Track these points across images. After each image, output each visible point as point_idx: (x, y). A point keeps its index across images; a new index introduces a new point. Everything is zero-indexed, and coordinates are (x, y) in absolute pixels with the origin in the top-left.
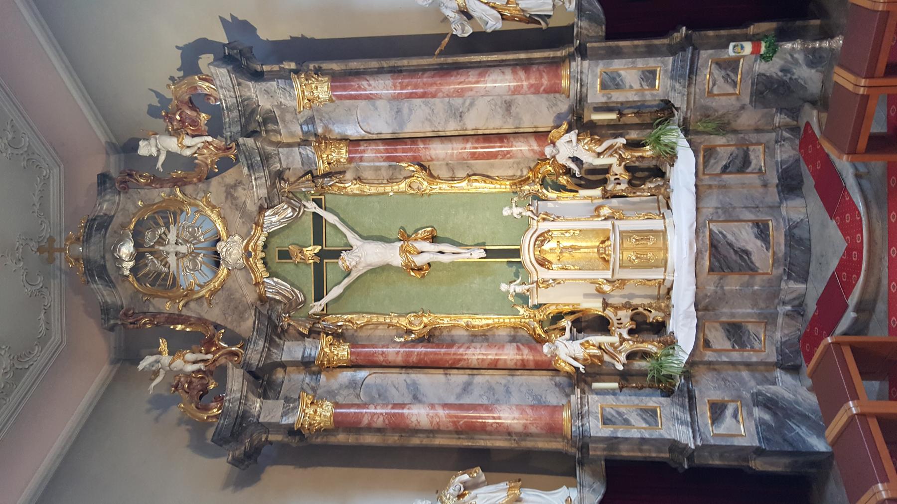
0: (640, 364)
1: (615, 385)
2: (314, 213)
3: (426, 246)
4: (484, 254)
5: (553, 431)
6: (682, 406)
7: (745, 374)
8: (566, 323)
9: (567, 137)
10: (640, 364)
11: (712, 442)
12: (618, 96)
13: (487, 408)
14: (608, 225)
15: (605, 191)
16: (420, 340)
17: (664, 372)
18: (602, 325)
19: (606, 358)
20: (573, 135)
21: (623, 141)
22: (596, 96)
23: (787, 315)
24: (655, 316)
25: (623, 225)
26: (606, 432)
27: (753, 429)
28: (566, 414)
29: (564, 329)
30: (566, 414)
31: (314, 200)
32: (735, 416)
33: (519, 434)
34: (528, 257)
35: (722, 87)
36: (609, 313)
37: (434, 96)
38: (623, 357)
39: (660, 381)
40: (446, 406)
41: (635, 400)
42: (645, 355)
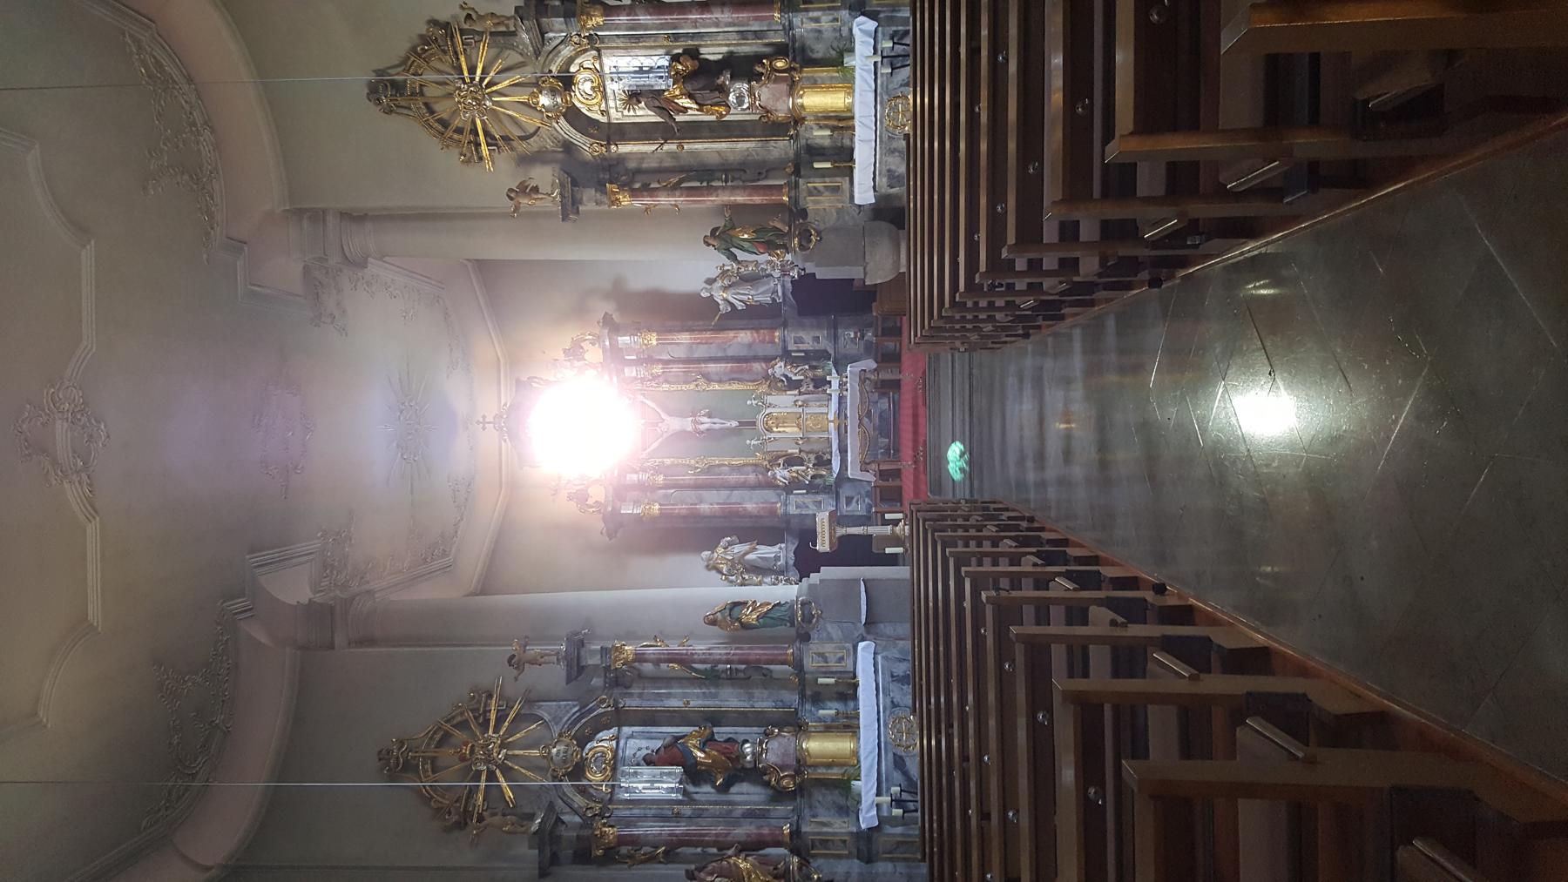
0: (818, 481)
1: (804, 491)
3: (706, 419)
4: (738, 424)
5: (773, 512)
8: (781, 461)
9: (779, 365)
10: (818, 481)
11: (845, 514)
12: (802, 347)
14: (801, 410)
16: (703, 472)
17: (827, 484)
18: (801, 462)
19: (800, 478)
21: (807, 367)
22: (791, 347)
23: (881, 453)
24: (826, 457)
25: (807, 410)
26: (797, 512)
27: (864, 507)
28: (779, 505)
29: (780, 464)
30: (779, 505)
32: (857, 502)
33: (756, 516)
34: (760, 426)
35: (854, 346)
36: (803, 455)
37: (711, 343)
38: (809, 478)
40: (718, 504)
41: (812, 496)
42: (822, 476)
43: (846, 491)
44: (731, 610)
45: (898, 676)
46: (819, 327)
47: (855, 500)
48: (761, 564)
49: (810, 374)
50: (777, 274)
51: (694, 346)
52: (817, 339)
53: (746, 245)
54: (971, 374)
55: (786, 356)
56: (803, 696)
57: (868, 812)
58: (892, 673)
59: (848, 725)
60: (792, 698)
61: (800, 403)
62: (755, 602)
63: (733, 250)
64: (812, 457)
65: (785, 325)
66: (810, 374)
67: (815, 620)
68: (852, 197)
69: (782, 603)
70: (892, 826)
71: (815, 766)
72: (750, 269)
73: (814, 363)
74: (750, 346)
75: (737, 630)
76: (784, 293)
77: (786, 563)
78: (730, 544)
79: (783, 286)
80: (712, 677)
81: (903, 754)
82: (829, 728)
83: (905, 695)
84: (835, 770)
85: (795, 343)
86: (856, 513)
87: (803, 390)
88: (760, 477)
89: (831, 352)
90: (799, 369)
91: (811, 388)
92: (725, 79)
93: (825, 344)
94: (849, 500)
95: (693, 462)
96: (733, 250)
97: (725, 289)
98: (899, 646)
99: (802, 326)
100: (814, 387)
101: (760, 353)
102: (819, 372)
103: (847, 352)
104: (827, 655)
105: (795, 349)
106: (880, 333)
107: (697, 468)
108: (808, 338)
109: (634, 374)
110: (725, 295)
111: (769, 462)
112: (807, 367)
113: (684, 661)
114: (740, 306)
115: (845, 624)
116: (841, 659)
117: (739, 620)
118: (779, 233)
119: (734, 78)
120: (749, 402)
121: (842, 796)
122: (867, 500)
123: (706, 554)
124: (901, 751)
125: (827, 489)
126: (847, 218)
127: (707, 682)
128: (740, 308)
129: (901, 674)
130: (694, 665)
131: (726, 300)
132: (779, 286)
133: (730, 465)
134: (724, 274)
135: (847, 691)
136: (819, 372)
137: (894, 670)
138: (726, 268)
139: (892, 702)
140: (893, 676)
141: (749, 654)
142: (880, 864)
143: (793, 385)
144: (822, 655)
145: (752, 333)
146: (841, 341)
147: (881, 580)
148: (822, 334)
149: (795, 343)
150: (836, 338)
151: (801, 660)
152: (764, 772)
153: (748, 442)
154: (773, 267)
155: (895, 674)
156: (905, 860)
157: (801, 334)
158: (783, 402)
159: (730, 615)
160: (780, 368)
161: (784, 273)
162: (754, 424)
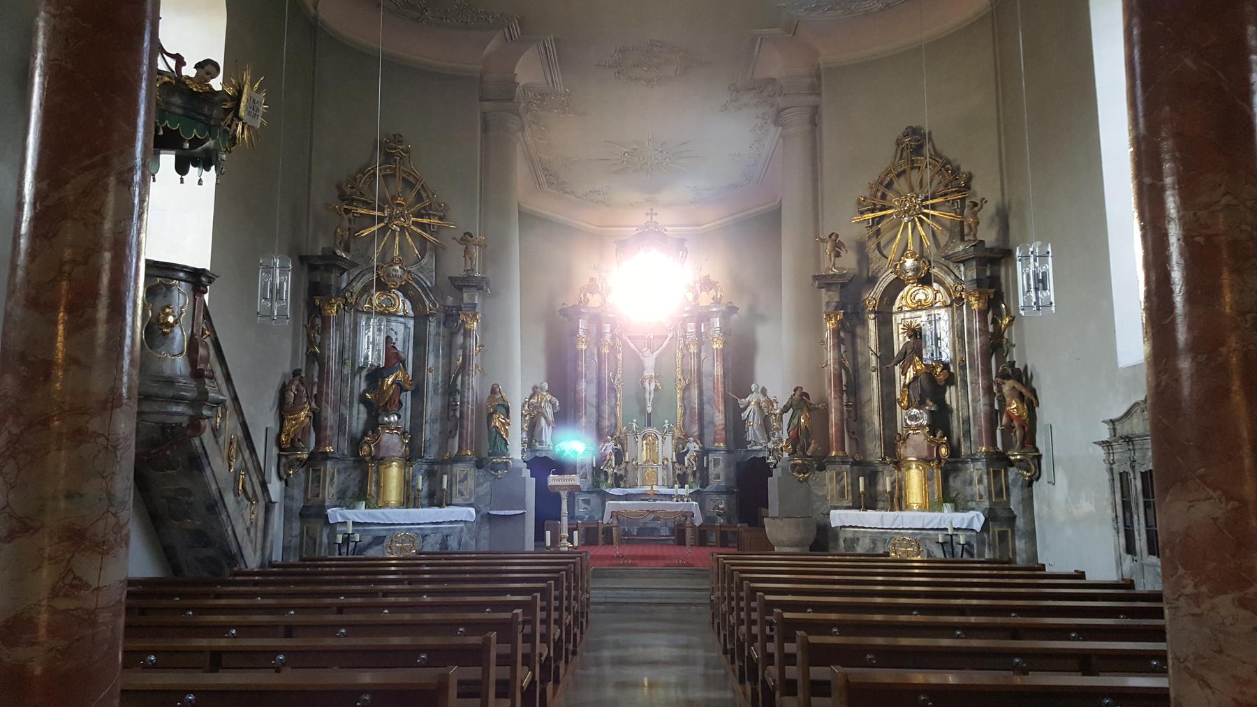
2: (667, 336)
3: (653, 387)
4: (649, 412)
6: (589, 489)
7: (600, 515)
8: (619, 447)
9: (697, 446)
10: (603, 476)
11: (576, 499)
12: (711, 465)
13: (585, 413)
14: (660, 463)
15: (675, 462)
18: (618, 462)
19: (605, 462)
20: (697, 449)
21: (695, 469)
23: (624, 529)
24: (622, 484)
25: (660, 469)
27: (581, 514)
31: (673, 336)
32: (585, 508)
34: (647, 430)
36: (623, 465)
37: (714, 392)
38: (605, 469)
39: (597, 482)
40: (585, 396)
42: (607, 480)
43: (595, 500)
44: (503, 406)
45: (447, 540)
46: (728, 479)
47: (587, 506)
48: (537, 430)
49: (689, 471)
50: (770, 445)
51: (712, 378)
52: (718, 477)
53: (795, 421)
54: (691, 604)
55: (704, 452)
56: (433, 463)
57: (340, 514)
58: (450, 535)
59: (409, 500)
60: (432, 454)
61: (666, 463)
62: (509, 425)
63: (791, 410)
64: (622, 472)
65: (729, 451)
66: (689, 471)
67: (493, 472)
68: (836, 508)
70: (328, 534)
71: (378, 472)
72: (775, 424)
73: (698, 475)
74: (712, 423)
75: (487, 409)
76: (754, 450)
77: (537, 450)
78: (554, 405)
79: (760, 450)
80: (450, 390)
81: (385, 544)
82: (407, 484)
83: (432, 546)
84: (374, 488)
85: (715, 459)
86: (576, 507)
87: (676, 465)
88: (607, 430)
89: (707, 489)
90: (694, 463)
91: (678, 472)
92: (930, 406)
93: (714, 484)
94: (587, 502)
95: (619, 376)
96: (791, 410)
97: (758, 403)
99: (728, 465)
100: (679, 474)
101: (706, 431)
102: (691, 479)
103: (707, 502)
104: (466, 483)
105: (710, 460)
106: (723, 529)
107: (614, 379)
108: (719, 472)
109: (689, 330)
110: (753, 403)
111: (619, 437)
112: (695, 469)
113: (464, 368)
114: (744, 415)
115: (489, 497)
116: (462, 494)
117: (495, 412)
118: (804, 449)
119: (931, 413)
120: (666, 421)
121: (353, 494)
122: (587, 516)
123: (546, 386)
124: (387, 542)
125: (596, 483)
126: (818, 503)
127: (447, 386)
128: (742, 415)
129: (449, 543)
130: (460, 377)
131: (749, 404)
132: (759, 447)
133: (616, 405)
134: (770, 403)
135: (436, 499)
136: (691, 479)
138: (775, 405)
139: (427, 536)
140: (447, 536)
141: (468, 420)
142: (299, 524)
143: (680, 457)
144: (465, 478)
145: (722, 424)
146: (715, 497)
147: (524, 528)
148: (722, 482)
149: (715, 459)
150: (718, 493)
152: (375, 431)
153: (635, 420)
154: (776, 443)
155: (448, 538)
156: (301, 544)
157: (722, 465)
158: (667, 449)
160: (694, 447)
161: (771, 452)
162: (649, 425)
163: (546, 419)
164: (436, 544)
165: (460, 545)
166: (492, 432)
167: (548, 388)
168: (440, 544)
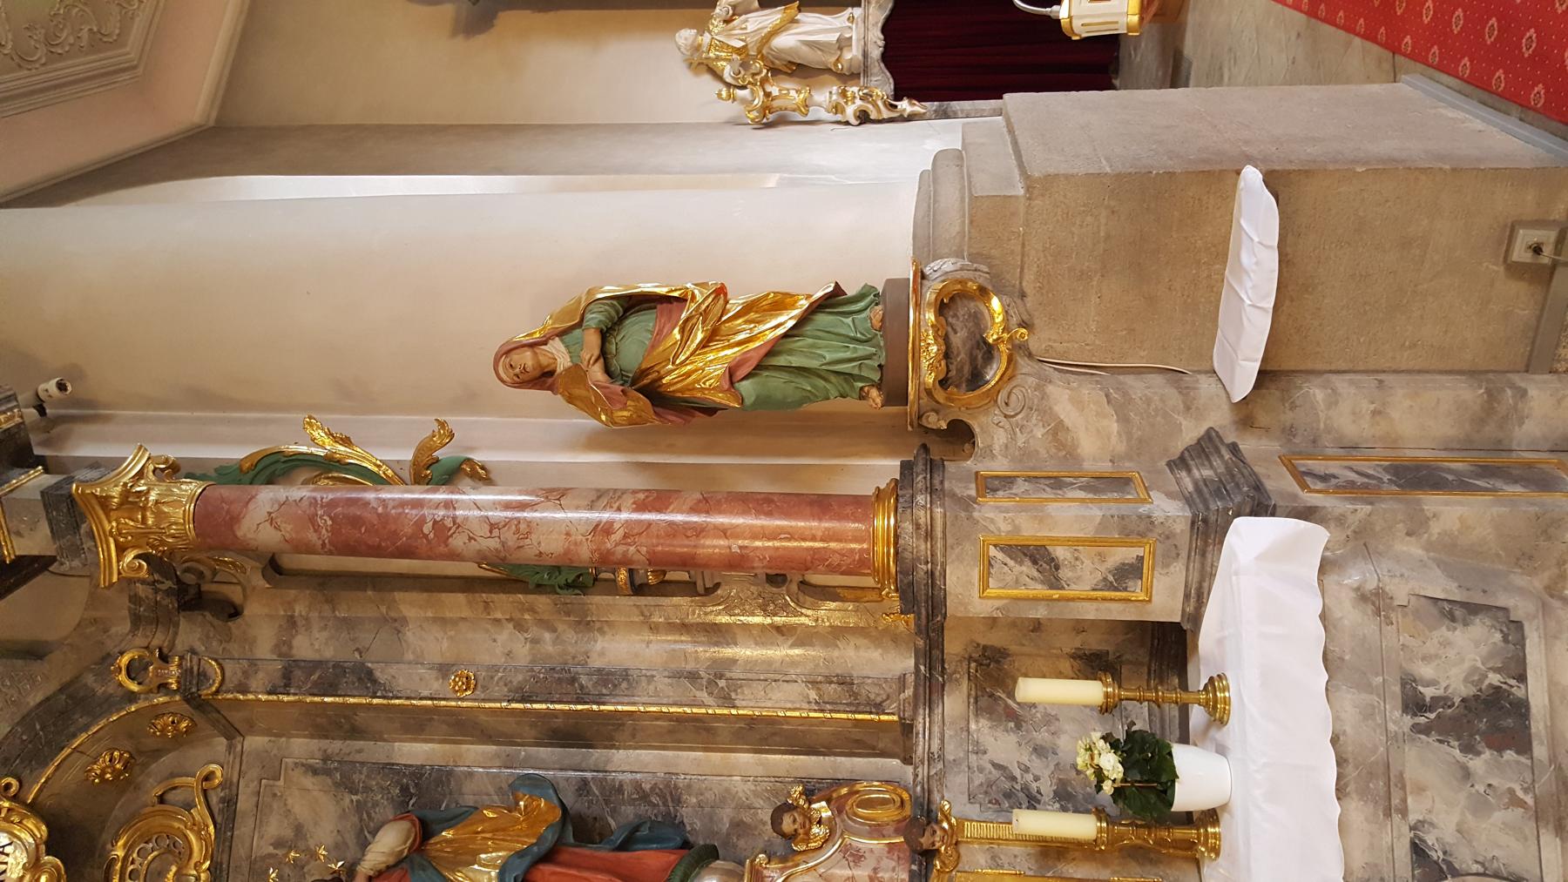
44: (606, 333)
45: (1444, 701)
58: (1409, 684)
62: (721, 291)
69: (851, 291)
83: (1480, 806)
98: (1435, 528)
129: (1467, 691)
137: (1426, 671)
140: (1414, 704)
141: (700, 531)
144: (1037, 555)
151: (934, 580)
155: (1428, 692)
159: (604, 353)
163: (775, 32)
164: (1467, 774)
165: (1473, 609)
166: (763, 402)
167: (691, 28)
168: (1469, 749)
